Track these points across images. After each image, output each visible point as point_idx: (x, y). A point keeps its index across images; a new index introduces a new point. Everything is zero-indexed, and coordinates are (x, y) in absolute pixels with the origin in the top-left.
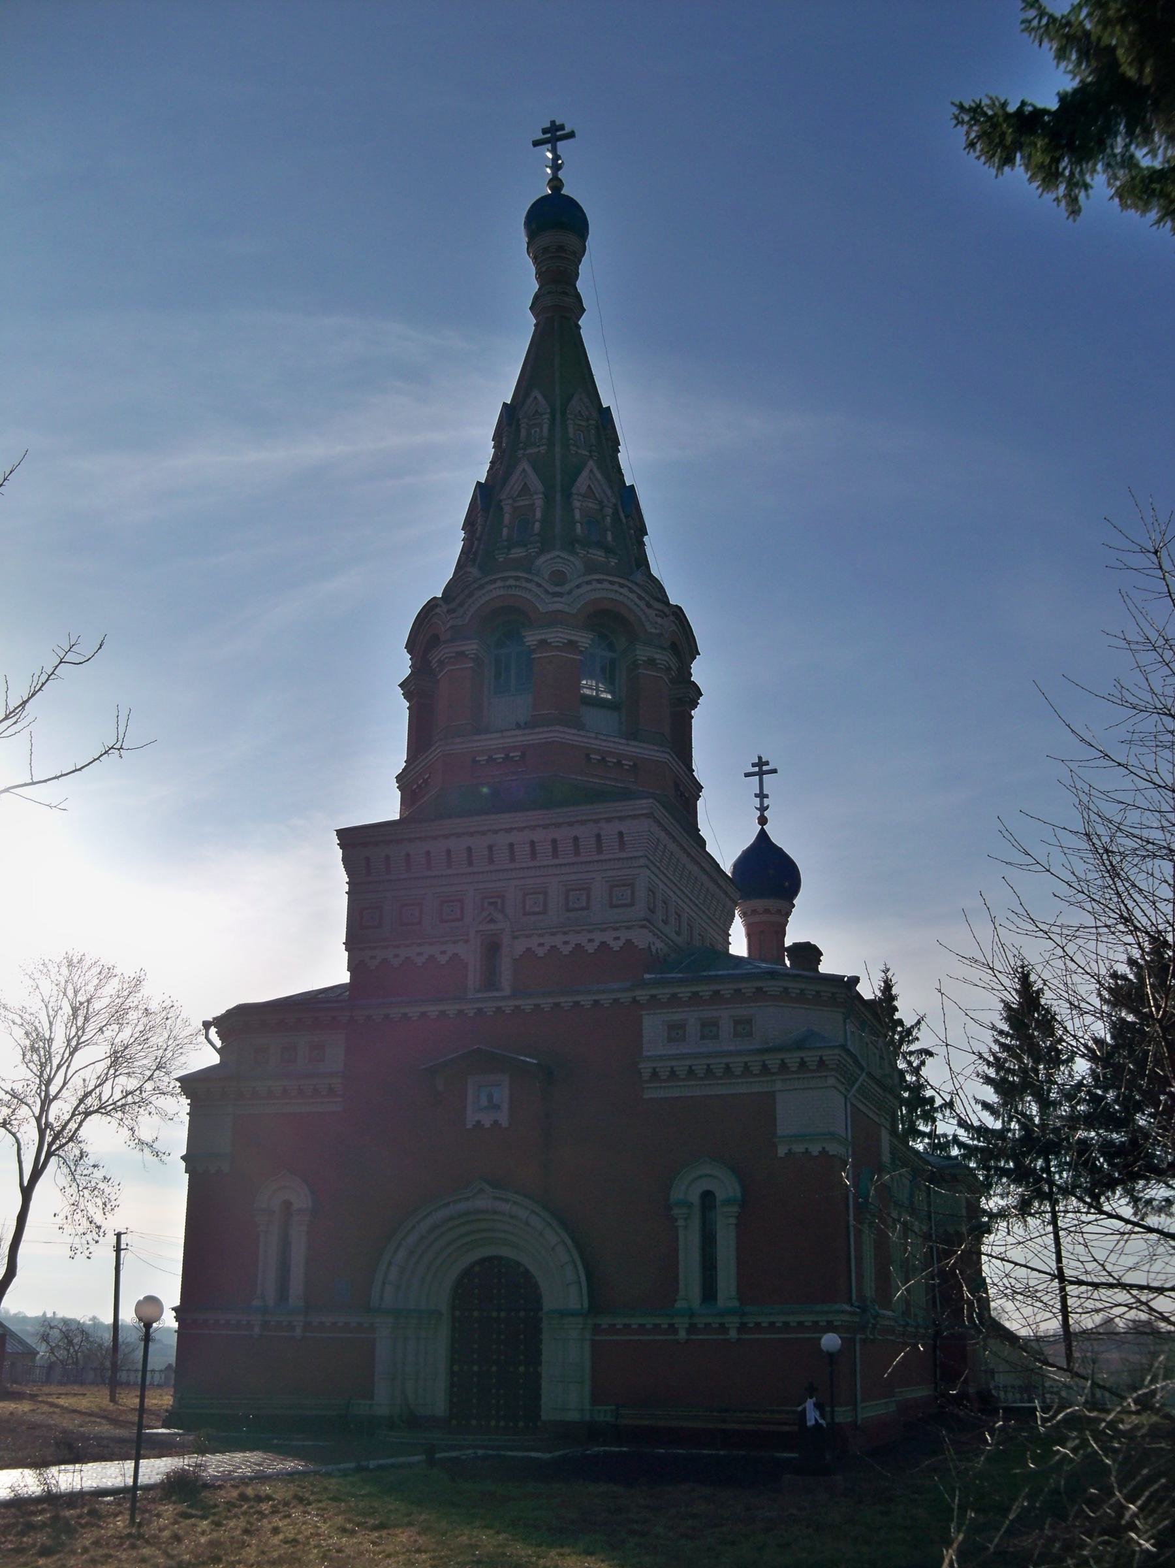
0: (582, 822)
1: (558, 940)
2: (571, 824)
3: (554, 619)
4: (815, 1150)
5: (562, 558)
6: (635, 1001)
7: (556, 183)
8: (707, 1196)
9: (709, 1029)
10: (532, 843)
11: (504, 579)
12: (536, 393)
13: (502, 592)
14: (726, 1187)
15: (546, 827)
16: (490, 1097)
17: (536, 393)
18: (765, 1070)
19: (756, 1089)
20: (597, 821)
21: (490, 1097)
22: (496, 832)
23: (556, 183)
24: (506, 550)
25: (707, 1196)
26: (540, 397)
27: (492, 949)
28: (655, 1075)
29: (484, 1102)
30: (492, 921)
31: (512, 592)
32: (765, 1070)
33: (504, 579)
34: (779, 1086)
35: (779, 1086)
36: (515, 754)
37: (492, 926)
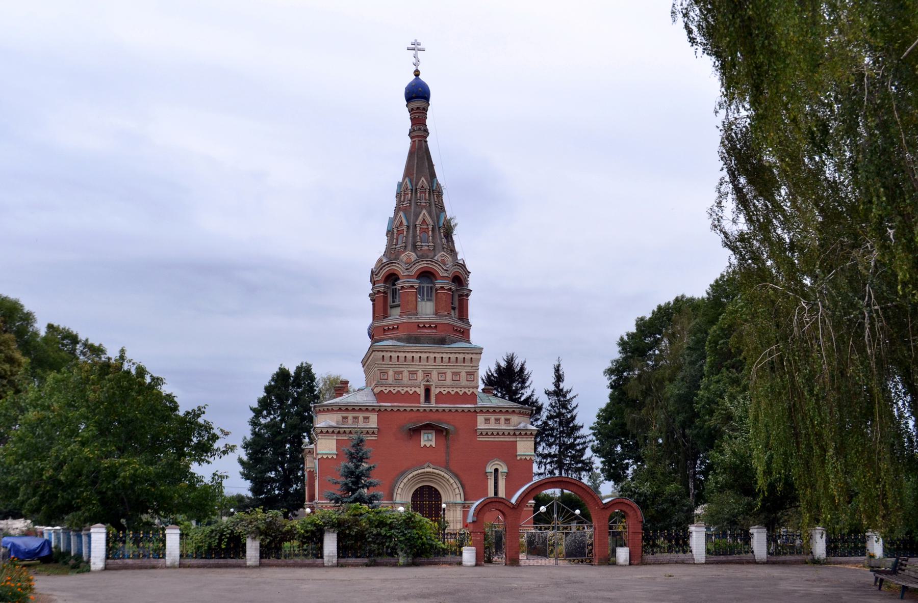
0: (459, 353)
1: (450, 390)
2: (455, 353)
3: (443, 278)
4: (524, 458)
6: (475, 411)
8: (496, 470)
9: (497, 420)
10: (442, 358)
11: (427, 261)
13: (425, 265)
14: (503, 469)
15: (447, 353)
16: (428, 437)
17: (423, 179)
18: (514, 434)
19: (511, 440)
20: (464, 353)
21: (428, 437)
22: (430, 352)
25: (496, 470)
26: (424, 180)
27: (428, 391)
28: (481, 434)
29: (426, 438)
30: (428, 381)
31: (430, 266)
32: (514, 434)
33: (427, 261)
34: (518, 439)
35: (518, 439)
37: (428, 383)
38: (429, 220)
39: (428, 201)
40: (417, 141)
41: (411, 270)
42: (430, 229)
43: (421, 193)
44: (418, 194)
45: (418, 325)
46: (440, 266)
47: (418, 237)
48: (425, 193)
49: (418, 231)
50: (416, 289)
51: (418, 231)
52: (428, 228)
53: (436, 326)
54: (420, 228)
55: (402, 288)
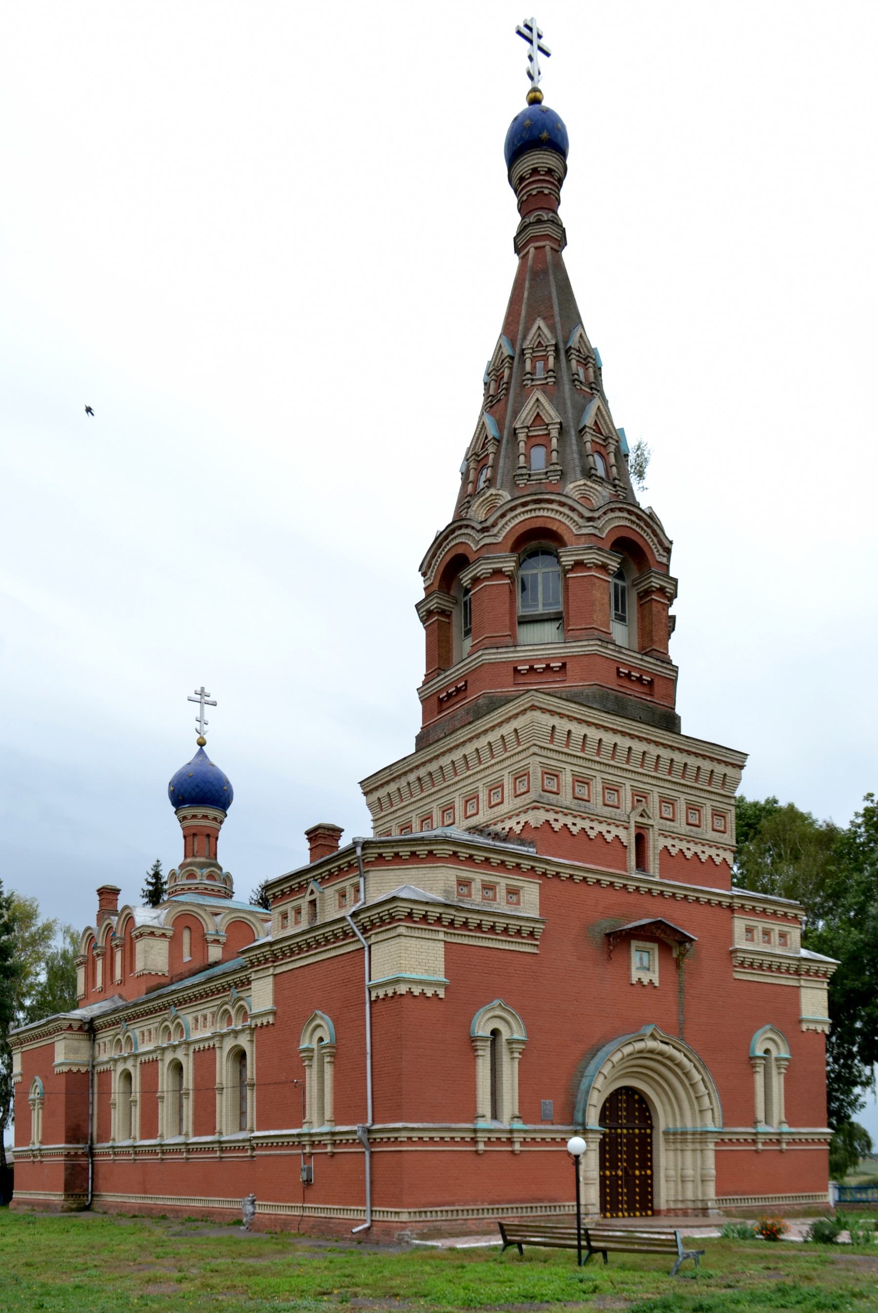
5: (588, 486)
7: (535, 100)
12: (540, 322)
17: (540, 322)
23: (535, 100)
24: (527, 477)
36: (555, 664)
38: (551, 414)
39: (551, 373)
40: (532, 250)
41: (495, 530)
42: (554, 433)
43: (534, 360)
44: (528, 362)
45: (515, 669)
46: (573, 509)
47: (522, 458)
48: (545, 359)
49: (522, 444)
50: (509, 577)
51: (522, 444)
52: (548, 434)
53: (564, 665)
54: (528, 437)
55: (476, 580)
